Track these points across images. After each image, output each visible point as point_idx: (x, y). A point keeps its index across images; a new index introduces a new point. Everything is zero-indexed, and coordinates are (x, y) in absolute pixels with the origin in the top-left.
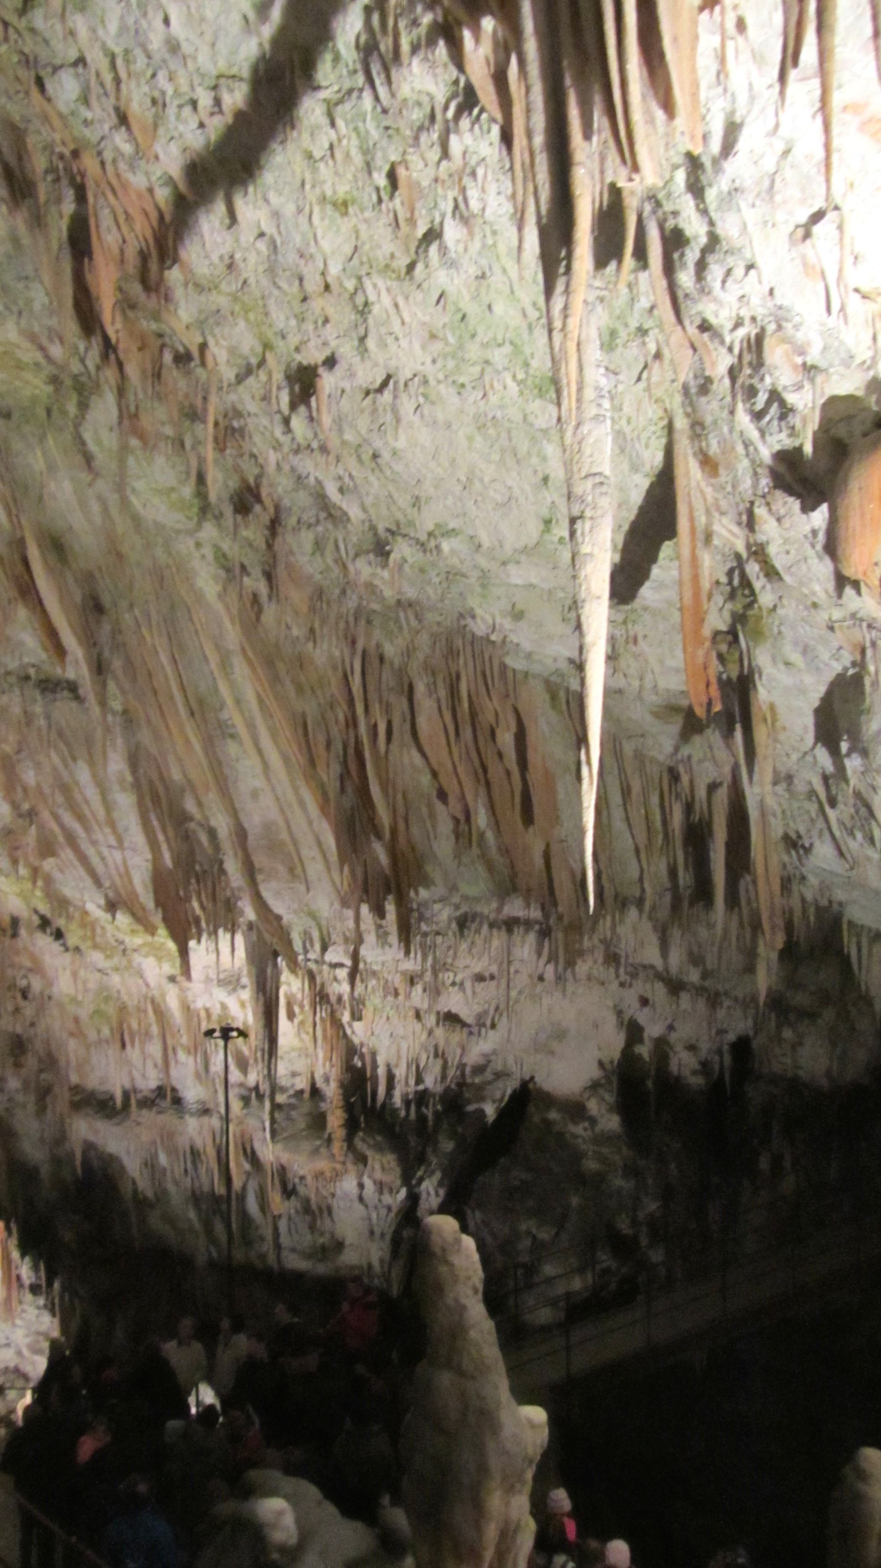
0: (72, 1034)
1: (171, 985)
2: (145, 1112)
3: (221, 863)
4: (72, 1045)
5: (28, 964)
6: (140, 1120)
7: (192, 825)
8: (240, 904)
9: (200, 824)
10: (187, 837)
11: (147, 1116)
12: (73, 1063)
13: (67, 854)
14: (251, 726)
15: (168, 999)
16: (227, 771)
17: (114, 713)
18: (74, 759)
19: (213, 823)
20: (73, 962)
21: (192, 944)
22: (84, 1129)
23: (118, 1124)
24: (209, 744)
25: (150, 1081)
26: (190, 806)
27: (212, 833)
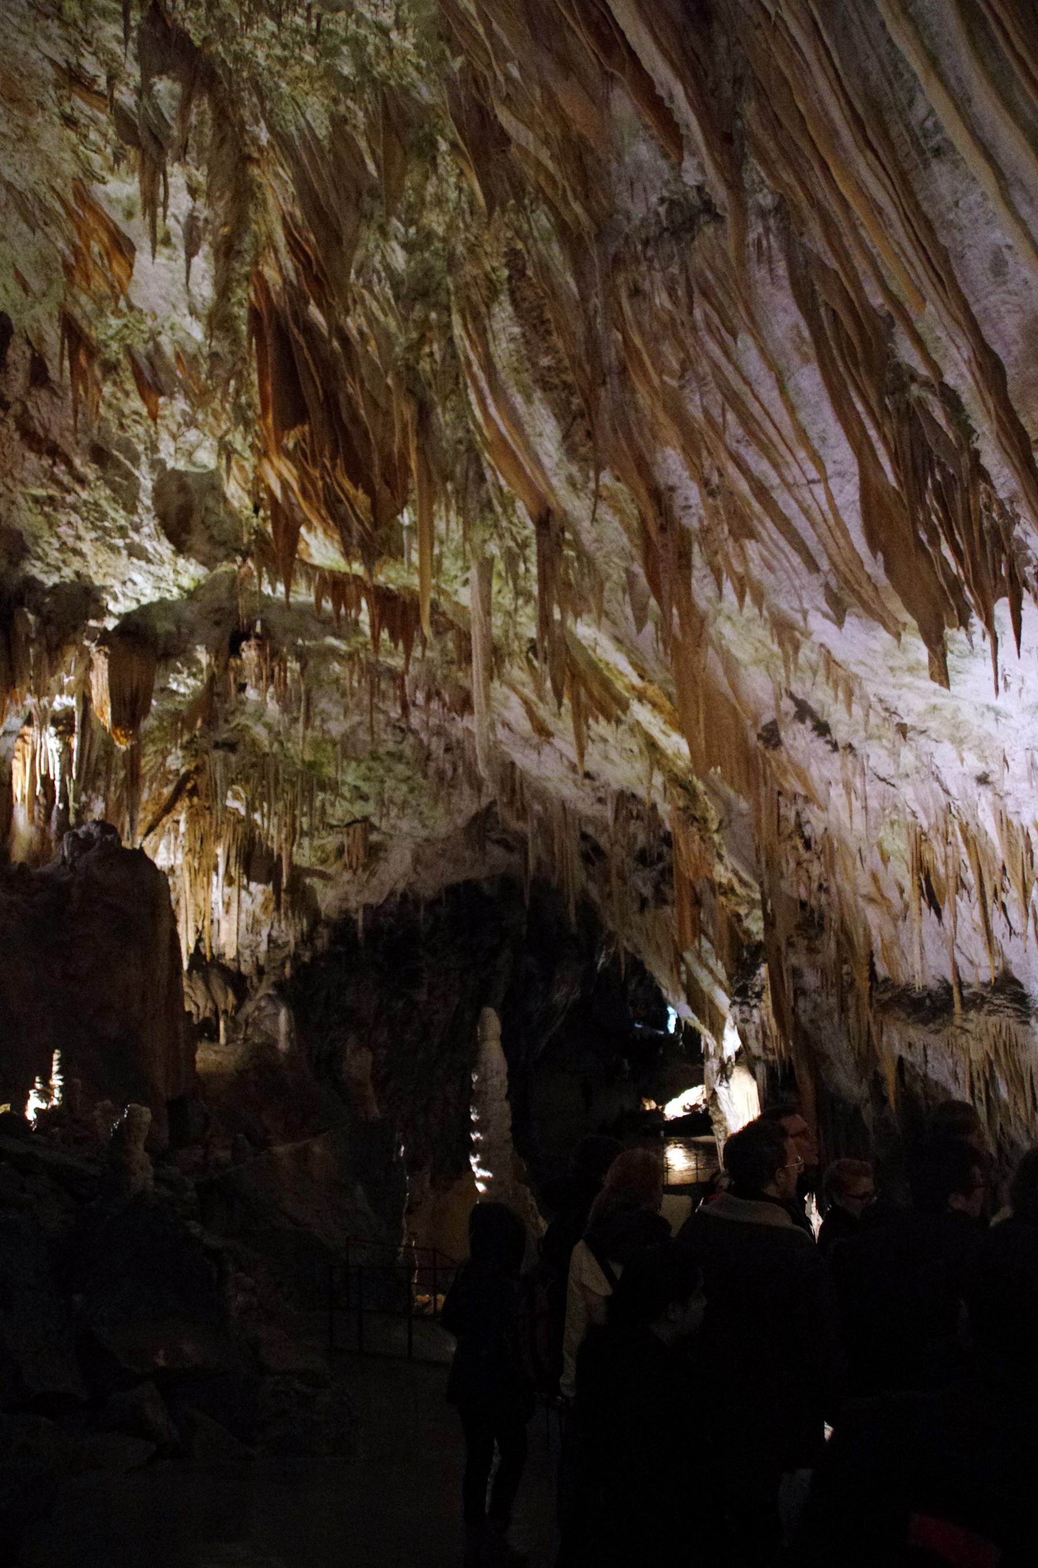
0: (871, 900)
1: (982, 789)
2: (972, 1014)
3: (976, 455)
4: (873, 915)
5: (800, 790)
6: (969, 1026)
7: (915, 389)
8: (1017, 531)
9: (926, 384)
10: (911, 416)
11: (976, 1020)
12: (877, 944)
13: (768, 529)
14: (961, 104)
15: (981, 815)
16: (944, 239)
17: (763, 214)
18: (734, 335)
19: (950, 379)
20: (844, 766)
21: (955, 636)
22: (898, 1039)
23: (937, 1032)
24: (905, 186)
25: (981, 971)
26: (907, 353)
27: (951, 399)
